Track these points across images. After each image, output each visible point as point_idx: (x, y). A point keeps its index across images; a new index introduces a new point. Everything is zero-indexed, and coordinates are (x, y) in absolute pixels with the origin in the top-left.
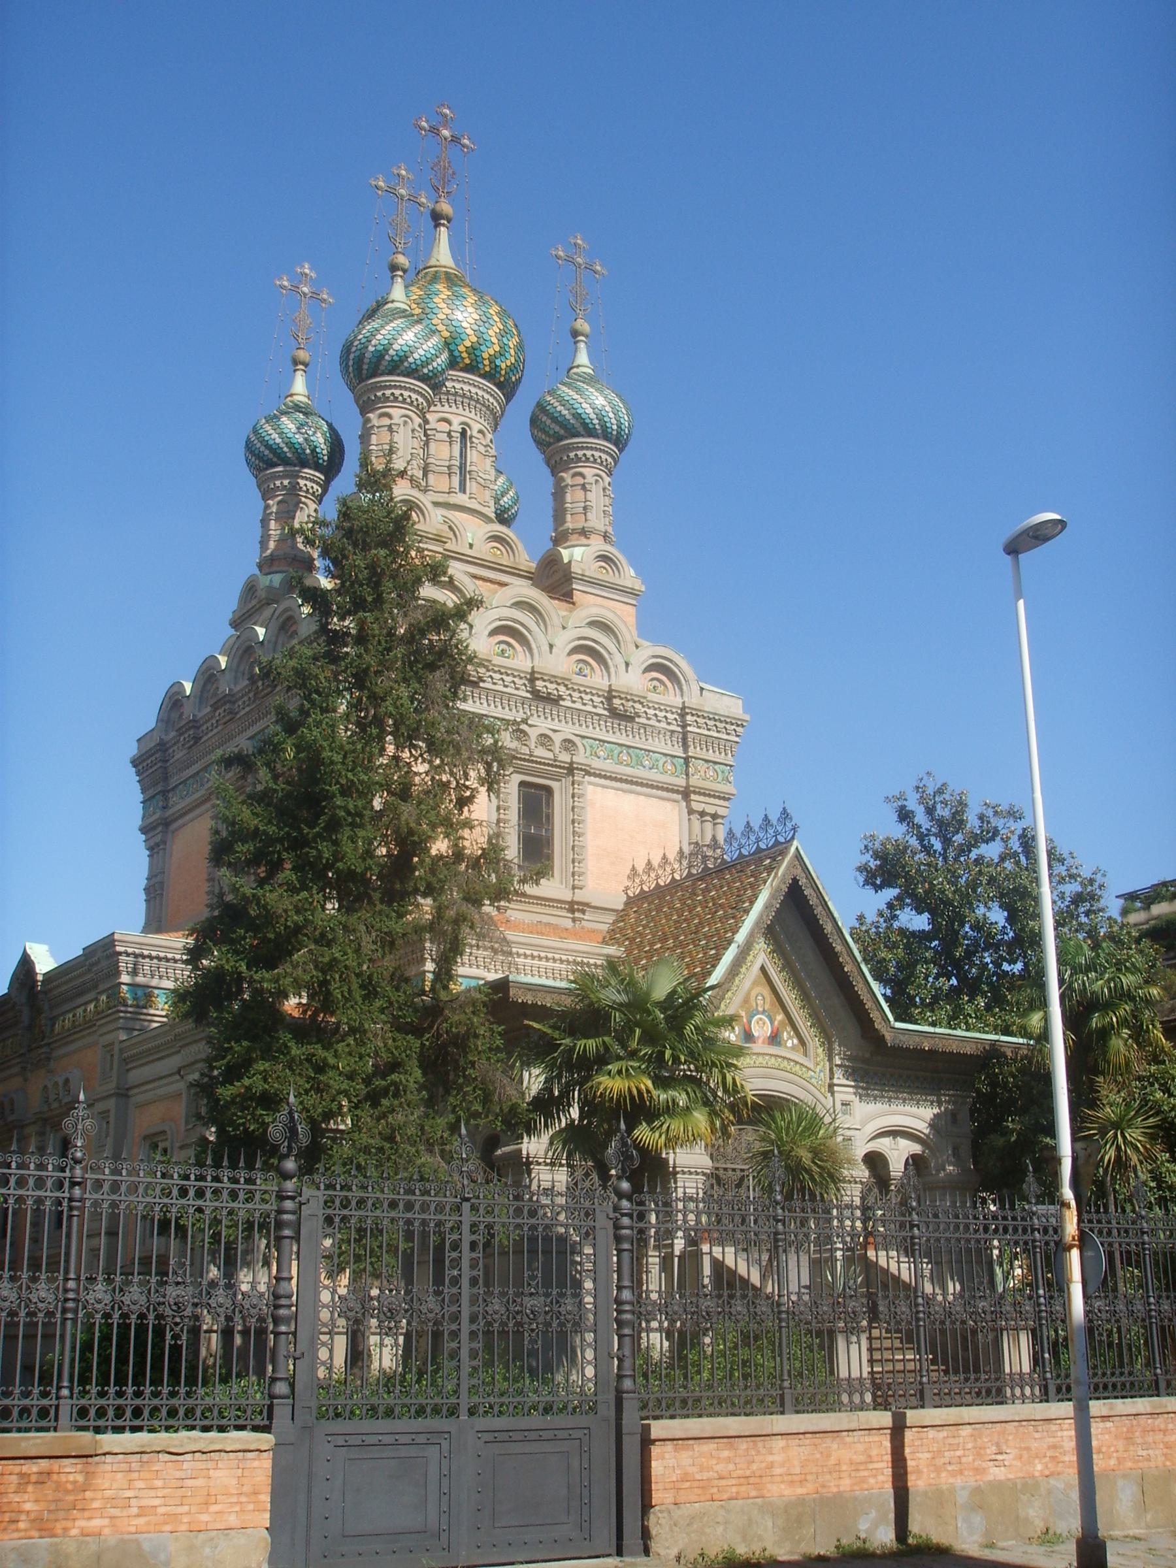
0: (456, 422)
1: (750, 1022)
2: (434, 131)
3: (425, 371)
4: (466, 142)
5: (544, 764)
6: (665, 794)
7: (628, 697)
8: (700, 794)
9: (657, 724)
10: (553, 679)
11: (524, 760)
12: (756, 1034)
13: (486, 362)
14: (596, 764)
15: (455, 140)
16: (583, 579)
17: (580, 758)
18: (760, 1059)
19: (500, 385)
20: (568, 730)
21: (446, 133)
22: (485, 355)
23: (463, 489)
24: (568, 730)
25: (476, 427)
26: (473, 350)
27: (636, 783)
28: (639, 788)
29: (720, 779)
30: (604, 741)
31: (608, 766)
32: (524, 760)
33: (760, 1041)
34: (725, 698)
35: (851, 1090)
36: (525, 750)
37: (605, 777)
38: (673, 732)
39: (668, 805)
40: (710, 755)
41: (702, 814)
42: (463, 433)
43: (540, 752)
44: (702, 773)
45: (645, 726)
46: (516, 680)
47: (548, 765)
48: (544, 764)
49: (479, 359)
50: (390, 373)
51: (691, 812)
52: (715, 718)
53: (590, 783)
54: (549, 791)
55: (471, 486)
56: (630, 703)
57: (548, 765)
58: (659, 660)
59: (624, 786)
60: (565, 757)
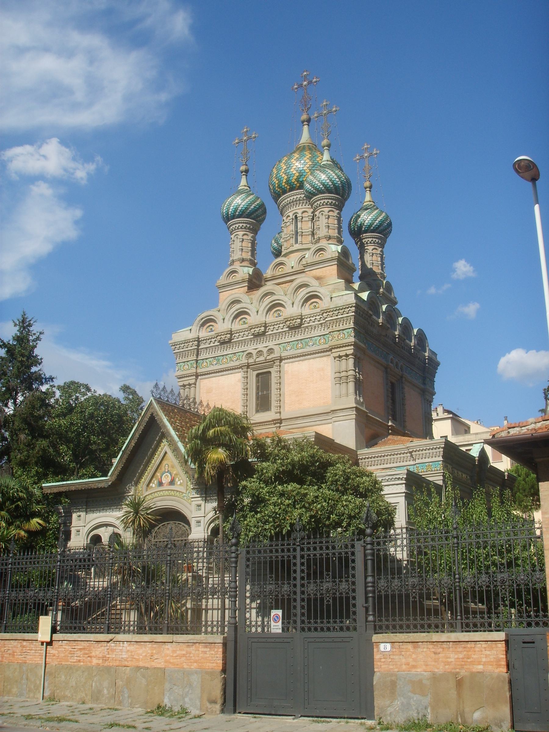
1: (161, 477)
2: (301, 86)
3: (237, 213)
4: (315, 80)
5: (262, 363)
6: (322, 354)
7: (291, 319)
8: (335, 348)
9: (314, 324)
10: (257, 326)
11: (253, 365)
12: (164, 482)
13: (296, 183)
15: (310, 83)
18: (161, 493)
20: (271, 344)
21: (305, 83)
22: (293, 181)
24: (271, 344)
25: (300, 212)
26: (287, 182)
27: (305, 355)
28: (309, 357)
29: (346, 336)
30: (289, 342)
32: (253, 365)
33: (165, 485)
34: (344, 296)
35: (200, 499)
37: (290, 358)
38: (321, 324)
39: (325, 358)
40: (341, 327)
43: (262, 358)
44: (336, 338)
45: (307, 327)
46: (311, 318)
47: (264, 363)
48: (262, 363)
49: (292, 184)
52: (338, 309)
53: (285, 363)
54: (270, 372)
56: (295, 321)
57: (264, 363)
58: (237, 312)
59: (302, 358)
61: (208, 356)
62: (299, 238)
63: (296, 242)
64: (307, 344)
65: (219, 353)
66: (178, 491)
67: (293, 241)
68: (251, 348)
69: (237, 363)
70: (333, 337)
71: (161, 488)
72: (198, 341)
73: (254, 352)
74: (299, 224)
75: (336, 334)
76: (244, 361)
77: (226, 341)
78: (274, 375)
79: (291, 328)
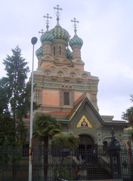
0: (59, 46)
7: (79, 79)
10: (67, 78)
14: (76, 89)
16: (75, 64)
17: (73, 88)
19: (65, 40)
20: (71, 85)
23: (60, 54)
25: (62, 46)
31: (77, 89)
36: (64, 88)
40: (94, 86)
41: (93, 94)
42: (60, 47)
50: (45, 41)
51: (91, 94)
54: (68, 93)
55: (61, 54)
60: (70, 88)
61: (46, 82)
62: (55, 54)
63: (55, 55)
64: (82, 88)
65: (51, 83)
66: (90, 129)
67: (59, 54)
68: (63, 84)
69: (58, 87)
70: (92, 88)
71: (83, 127)
72: (44, 76)
73: (65, 86)
74: (56, 50)
75: (92, 87)
76: (61, 87)
77: (54, 79)
78: (70, 95)
79: (78, 81)
